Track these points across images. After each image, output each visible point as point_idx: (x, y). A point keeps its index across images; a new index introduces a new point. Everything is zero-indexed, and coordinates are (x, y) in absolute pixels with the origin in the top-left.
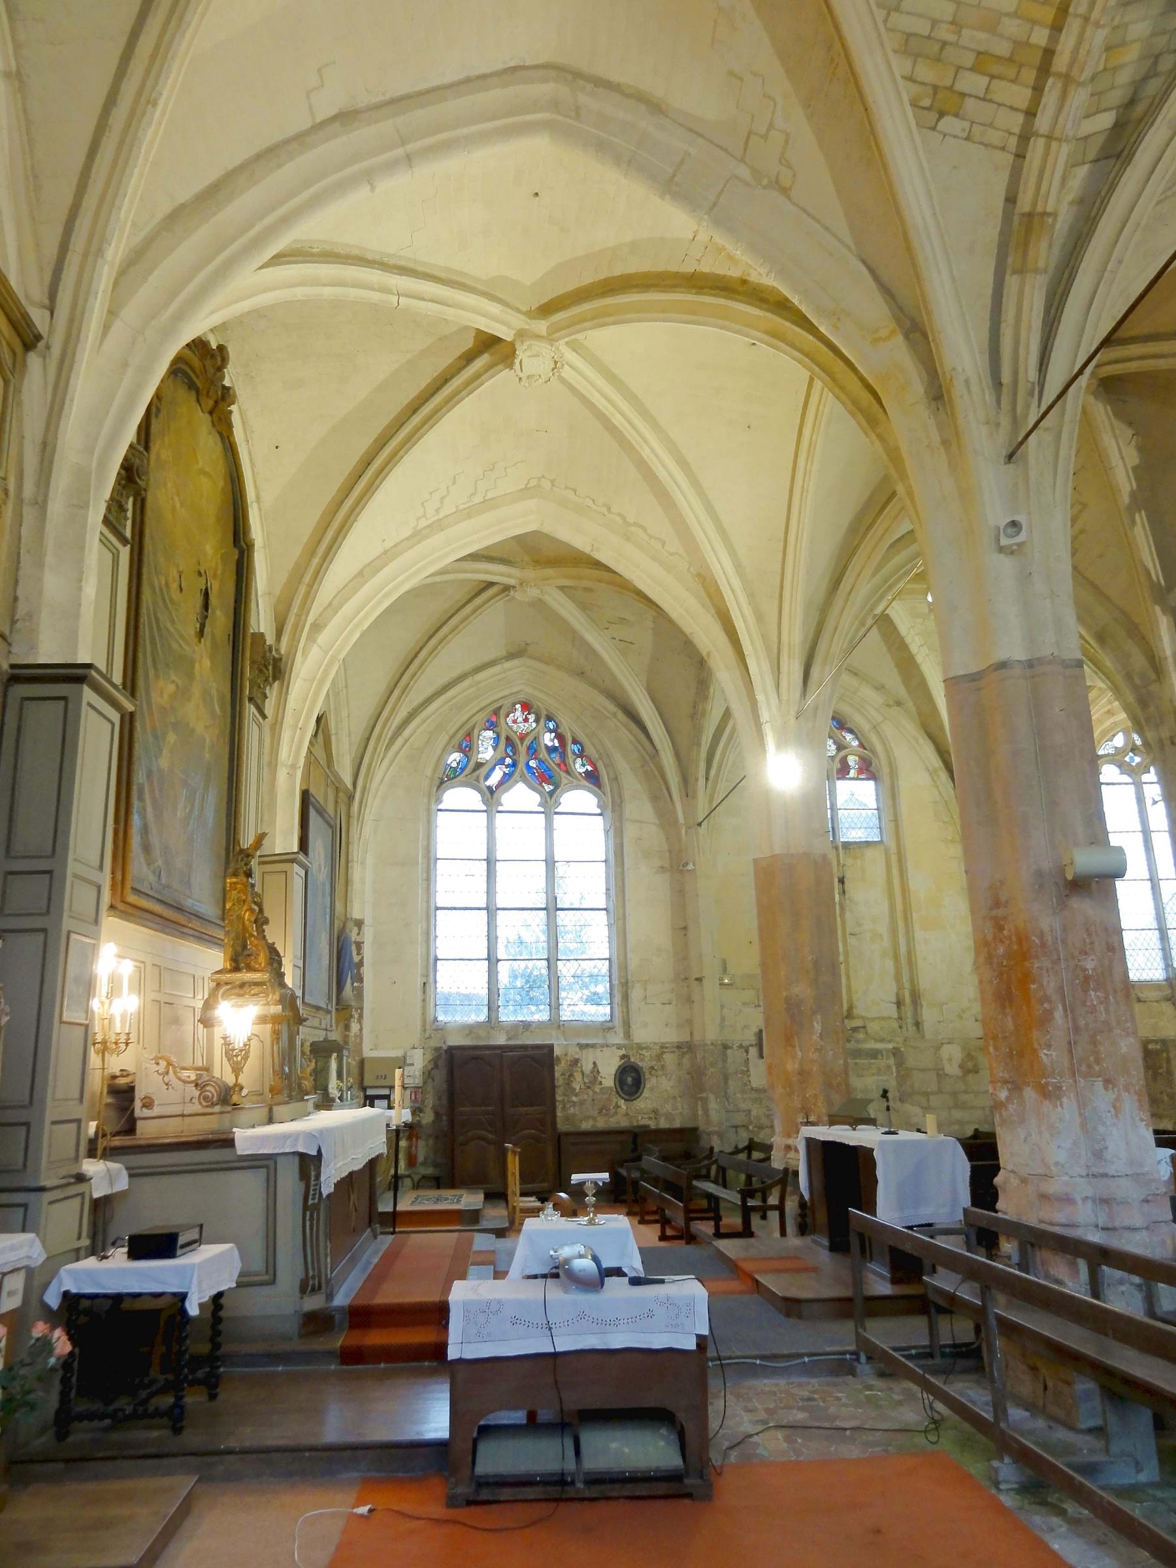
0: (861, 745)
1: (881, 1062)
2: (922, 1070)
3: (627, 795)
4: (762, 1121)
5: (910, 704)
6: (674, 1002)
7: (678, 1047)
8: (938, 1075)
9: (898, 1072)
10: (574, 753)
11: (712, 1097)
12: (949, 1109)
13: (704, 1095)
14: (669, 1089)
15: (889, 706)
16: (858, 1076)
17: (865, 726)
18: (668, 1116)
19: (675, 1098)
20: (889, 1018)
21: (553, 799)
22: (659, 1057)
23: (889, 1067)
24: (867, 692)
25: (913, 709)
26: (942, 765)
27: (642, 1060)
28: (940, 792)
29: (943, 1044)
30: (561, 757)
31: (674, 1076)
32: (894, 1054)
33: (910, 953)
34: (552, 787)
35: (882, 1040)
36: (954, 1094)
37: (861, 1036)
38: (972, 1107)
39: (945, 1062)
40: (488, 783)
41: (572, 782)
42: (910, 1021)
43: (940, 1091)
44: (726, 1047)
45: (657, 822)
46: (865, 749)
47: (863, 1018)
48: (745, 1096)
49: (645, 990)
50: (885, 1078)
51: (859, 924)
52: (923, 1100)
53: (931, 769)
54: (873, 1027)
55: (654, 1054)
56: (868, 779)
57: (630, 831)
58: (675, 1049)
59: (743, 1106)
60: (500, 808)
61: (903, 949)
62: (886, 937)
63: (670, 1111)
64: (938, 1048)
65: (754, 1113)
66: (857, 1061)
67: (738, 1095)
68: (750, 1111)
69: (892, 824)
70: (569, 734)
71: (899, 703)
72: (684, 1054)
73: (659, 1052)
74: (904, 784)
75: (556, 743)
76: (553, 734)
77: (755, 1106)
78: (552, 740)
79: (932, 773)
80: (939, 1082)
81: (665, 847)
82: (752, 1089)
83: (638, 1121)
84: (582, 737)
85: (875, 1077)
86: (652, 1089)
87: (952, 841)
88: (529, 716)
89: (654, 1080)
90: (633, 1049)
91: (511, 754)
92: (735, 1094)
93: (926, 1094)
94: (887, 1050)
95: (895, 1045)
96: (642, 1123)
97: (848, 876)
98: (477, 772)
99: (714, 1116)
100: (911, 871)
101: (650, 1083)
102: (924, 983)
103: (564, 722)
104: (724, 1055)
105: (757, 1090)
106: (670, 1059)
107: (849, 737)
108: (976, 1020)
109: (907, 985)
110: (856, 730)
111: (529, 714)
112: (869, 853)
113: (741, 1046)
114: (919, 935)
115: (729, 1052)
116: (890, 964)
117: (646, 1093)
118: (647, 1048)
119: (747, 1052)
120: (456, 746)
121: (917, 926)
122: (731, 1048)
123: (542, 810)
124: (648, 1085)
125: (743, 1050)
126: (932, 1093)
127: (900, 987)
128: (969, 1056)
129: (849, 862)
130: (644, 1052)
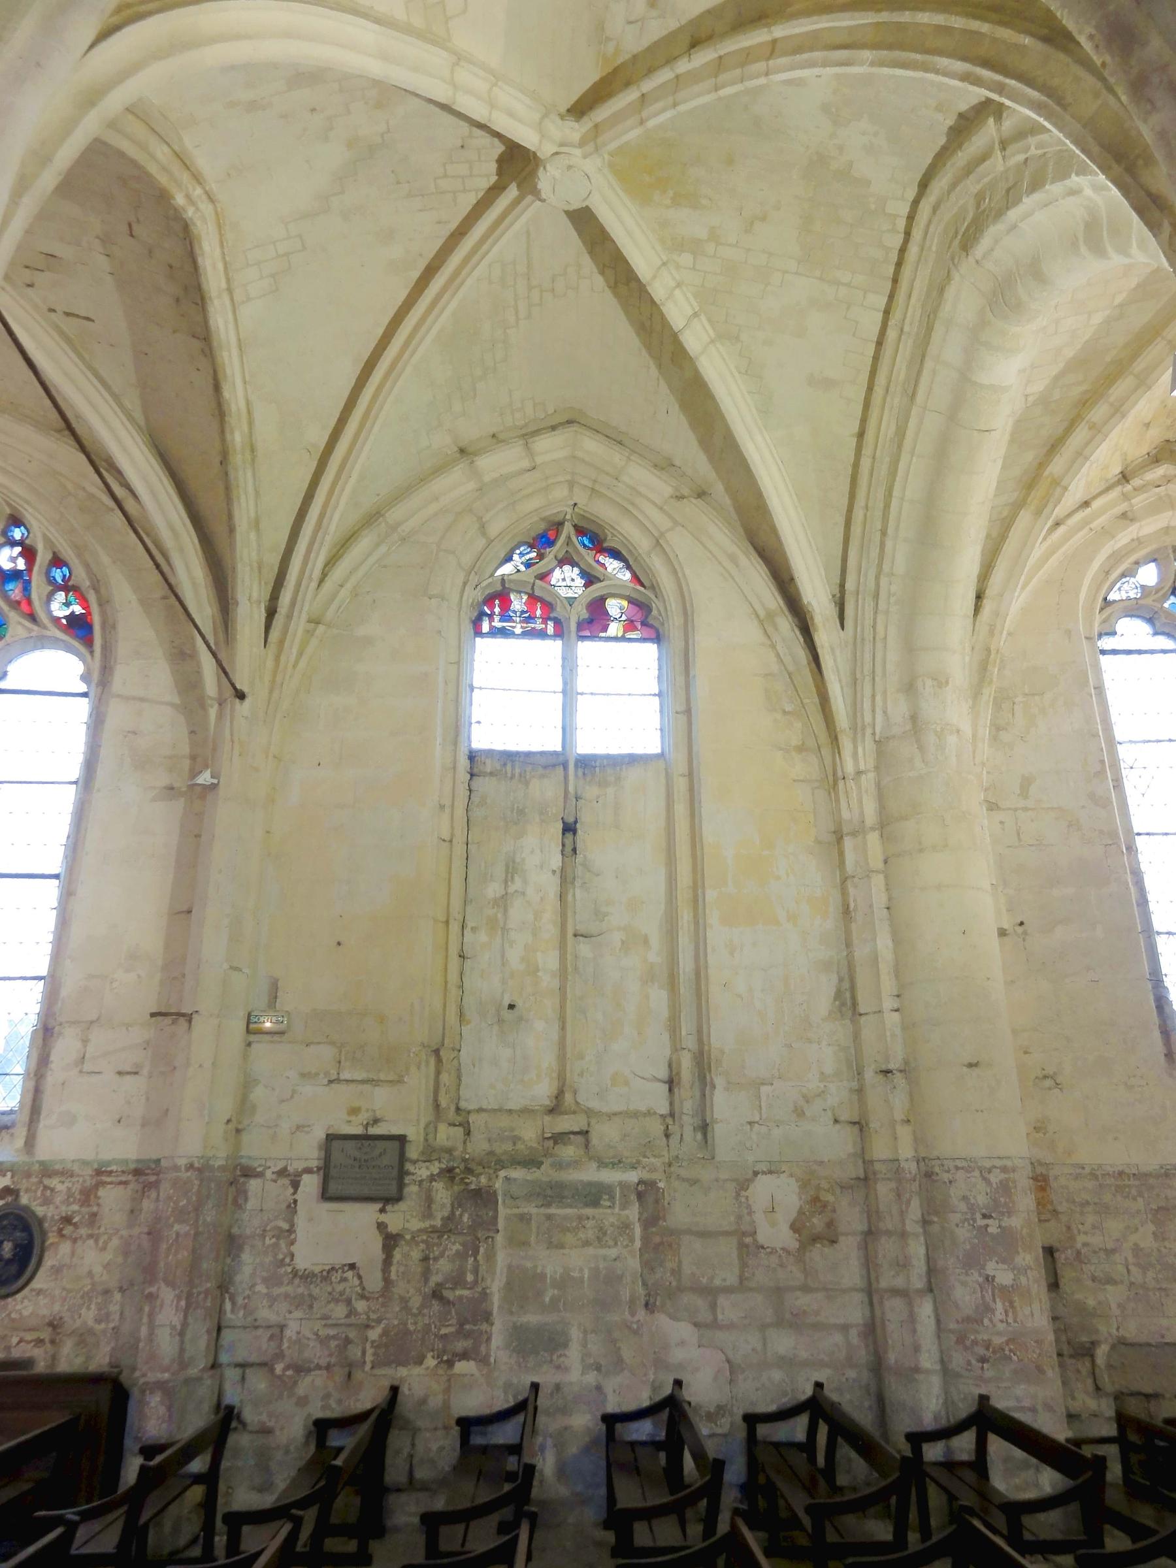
0: (636, 578)
1: (608, 1215)
2: (703, 1234)
3: (123, 649)
4: (307, 1354)
5: (719, 490)
6: (145, 1071)
7: (137, 1172)
8: (742, 1246)
9: (645, 1239)
10: (51, 581)
11: (167, 1295)
12: (763, 1328)
13: (153, 1289)
14: (98, 1269)
15: (680, 498)
16: (551, 1245)
17: (640, 542)
18: (84, 1338)
19: (107, 1292)
20: (649, 1113)
22: (88, 1195)
23: (626, 1227)
24: (639, 474)
25: (727, 502)
26: (781, 602)
27: (46, 1202)
28: (778, 655)
29: (756, 1174)
31: (115, 1242)
32: (640, 1196)
33: (699, 975)
35: (617, 1163)
36: (778, 1292)
37: (569, 1152)
38: (817, 1327)
39: (759, 1217)
42: (689, 1121)
43: (742, 1285)
44: (249, 1173)
45: (177, 700)
46: (642, 585)
47: (589, 1113)
48: (277, 1291)
49: (85, 1042)
50: (613, 1252)
51: (599, 915)
52: (700, 1303)
53: (762, 614)
54: (605, 1134)
55: (76, 1188)
56: (643, 640)
57: (117, 715)
58: (130, 1177)
59: (266, 1314)
61: (686, 964)
62: (655, 940)
63: (91, 1323)
64: (743, 1185)
65: (289, 1333)
66: (552, 1210)
67: (261, 1288)
68: (282, 1327)
69: (683, 718)
71: (701, 494)
72: (148, 1186)
73: (89, 1182)
74: (704, 641)
75: (21, 564)
76: (18, 549)
77: (298, 1314)
79: (765, 622)
80: (744, 1265)
81: (186, 749)
82: (295, 1273)
83: (8, 1348)
84: (68, 553)
85: (591, 1251)
86: (57, 1270)
87: (801, 749)
89: (65, 1248)
90: (28, 1175)
92: (253, 1286)
93: (711, 1293)
94: (623, 1185)
95: (646, 1176)
96: (16, 1354)
97: (586, 819)
99: (166, 1344)
100: (708, 806)
101: (57, 1253)
102: (721, 1037)
104: (242, 1193)
105: (307, 1277)
106: (112, 1199)
107: (612, 565)
108: (836, 1121)
109: (690, 1042)
110: (624, 553)
112: (633, 775)
113: (282, 1173)
114: (717, 935)
115: (254, 1185)
116: (659, 997)
117: (36, 1284)
118: (66, 1174)
119: (296, 1185)
121: (713, 918)
122: (260, 1175)
124: (49, 1262)
125: (286, 1181)
126: (729, 1290)
127: (676, 1048)
128: (817, 1203)
129: (591, 792)
130: (54, 1182)
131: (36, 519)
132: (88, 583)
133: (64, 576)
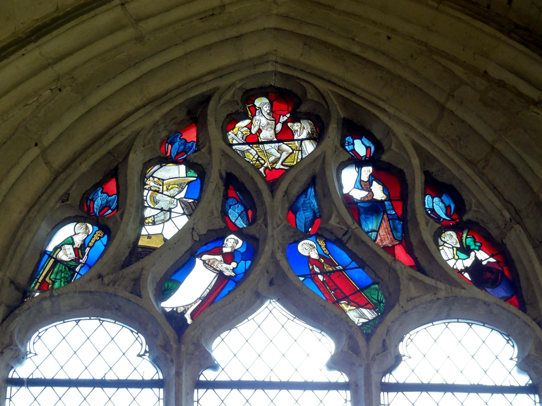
21: (376, 342)
30: (393, 229)
34: (369, 314)
40: (169, 304)
41: (436, 289)
60: (208, 375)
70: (416, 162)
76: (367, 171)
78: (366, 186)
88: (295, 127)
91: (240, 224)
98: (135, 267)
103: (399, 131)
111: (295, 119)
120: (76, 196)
123: (343, 378)
131: (400, 121)
132: (507, 215)
133: (448, 208)
